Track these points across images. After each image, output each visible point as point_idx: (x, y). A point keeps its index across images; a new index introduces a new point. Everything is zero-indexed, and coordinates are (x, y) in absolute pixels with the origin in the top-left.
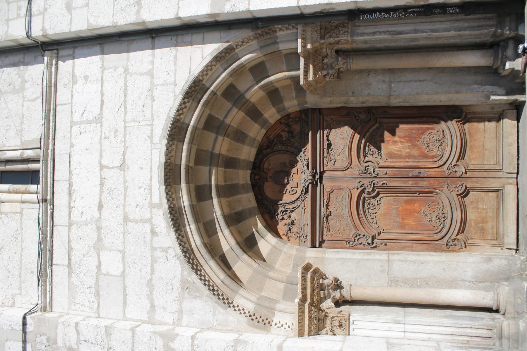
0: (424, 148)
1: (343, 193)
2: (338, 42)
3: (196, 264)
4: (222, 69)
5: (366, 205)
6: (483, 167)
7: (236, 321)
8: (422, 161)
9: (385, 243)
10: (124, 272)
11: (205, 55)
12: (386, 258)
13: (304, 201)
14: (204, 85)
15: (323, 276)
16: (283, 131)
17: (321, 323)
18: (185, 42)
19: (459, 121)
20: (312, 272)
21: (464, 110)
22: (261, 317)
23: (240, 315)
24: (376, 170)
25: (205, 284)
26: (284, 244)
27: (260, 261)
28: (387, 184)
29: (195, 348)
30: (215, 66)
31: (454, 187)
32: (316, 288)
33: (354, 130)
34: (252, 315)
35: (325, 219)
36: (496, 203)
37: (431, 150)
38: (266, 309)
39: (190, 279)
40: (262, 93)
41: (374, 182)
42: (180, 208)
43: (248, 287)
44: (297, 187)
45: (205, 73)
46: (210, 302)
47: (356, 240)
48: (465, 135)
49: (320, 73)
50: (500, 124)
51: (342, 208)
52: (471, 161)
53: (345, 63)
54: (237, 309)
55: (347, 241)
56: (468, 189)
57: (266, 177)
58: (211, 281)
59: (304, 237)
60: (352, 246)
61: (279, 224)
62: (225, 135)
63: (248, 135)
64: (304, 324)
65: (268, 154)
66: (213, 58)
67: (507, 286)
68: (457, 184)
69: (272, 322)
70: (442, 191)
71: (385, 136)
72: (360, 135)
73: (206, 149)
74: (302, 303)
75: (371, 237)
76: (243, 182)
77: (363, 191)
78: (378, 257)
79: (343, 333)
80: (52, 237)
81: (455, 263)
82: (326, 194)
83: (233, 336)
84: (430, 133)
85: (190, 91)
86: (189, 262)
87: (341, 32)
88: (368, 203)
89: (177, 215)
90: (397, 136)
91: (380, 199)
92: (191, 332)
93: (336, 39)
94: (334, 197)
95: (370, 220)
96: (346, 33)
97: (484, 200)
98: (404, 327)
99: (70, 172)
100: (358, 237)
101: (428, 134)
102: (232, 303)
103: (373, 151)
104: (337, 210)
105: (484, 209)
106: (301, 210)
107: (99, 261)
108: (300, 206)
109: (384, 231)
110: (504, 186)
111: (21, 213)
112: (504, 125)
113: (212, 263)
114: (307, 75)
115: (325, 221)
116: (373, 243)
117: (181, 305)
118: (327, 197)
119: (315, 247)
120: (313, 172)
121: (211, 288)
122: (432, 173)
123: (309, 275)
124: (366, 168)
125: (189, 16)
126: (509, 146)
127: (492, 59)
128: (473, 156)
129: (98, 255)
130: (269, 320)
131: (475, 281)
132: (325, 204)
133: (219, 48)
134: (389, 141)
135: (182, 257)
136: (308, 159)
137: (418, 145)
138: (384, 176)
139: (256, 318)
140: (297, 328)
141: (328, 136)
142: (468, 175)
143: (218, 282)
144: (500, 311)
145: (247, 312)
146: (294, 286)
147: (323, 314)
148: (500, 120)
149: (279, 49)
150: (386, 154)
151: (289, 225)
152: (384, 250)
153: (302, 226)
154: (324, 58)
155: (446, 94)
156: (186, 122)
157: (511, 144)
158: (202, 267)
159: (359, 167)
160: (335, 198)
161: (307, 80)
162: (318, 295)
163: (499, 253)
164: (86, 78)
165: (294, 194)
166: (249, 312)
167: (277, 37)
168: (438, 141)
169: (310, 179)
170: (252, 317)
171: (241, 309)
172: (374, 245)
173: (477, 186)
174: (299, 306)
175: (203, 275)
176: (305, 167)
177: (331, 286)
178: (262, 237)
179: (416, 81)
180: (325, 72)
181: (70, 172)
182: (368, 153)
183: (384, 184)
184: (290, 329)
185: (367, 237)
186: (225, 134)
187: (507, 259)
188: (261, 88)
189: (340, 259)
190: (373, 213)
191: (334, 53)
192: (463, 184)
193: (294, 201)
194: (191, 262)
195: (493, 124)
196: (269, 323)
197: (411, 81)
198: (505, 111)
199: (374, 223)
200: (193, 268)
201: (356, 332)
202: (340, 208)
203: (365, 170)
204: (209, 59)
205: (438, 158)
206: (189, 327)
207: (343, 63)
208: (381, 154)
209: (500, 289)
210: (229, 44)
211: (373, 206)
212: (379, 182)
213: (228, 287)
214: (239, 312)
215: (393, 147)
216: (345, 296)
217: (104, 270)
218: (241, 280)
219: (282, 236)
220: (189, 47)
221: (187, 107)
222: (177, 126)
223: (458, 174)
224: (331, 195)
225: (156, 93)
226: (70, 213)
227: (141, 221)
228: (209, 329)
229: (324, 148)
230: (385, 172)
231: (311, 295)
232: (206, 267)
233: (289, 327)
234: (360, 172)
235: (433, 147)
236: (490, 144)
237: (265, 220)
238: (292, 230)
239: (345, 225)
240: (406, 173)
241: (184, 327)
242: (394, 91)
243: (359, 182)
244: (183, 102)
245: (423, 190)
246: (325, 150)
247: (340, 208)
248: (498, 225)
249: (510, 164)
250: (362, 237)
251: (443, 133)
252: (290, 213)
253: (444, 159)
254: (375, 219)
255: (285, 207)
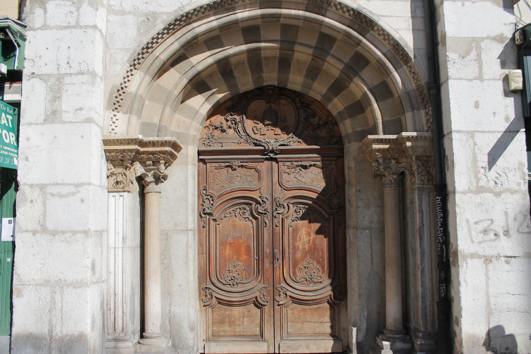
0: (303, 264)
1: (256, 182)
2: (412, 174)
3: (175, 28)
4: (385, 51)
5: (243, 206)
6: (285, 321)
7: (116, 73)
8: (290, 262)
9: (205, 226)
11: (400, 32)
12: (190, 228)
13: (247, 142)
14: (368, 32)
15: (168, 164)
16: (320, 119)
17: (119, 163)
18: (415, 10)
19: (331, 298)
20: (171, 151)
21: (343, 302)
22: (122, 99)
23: (123, 77)
24: (281, 215)
25: (153, 39)
26: (200, 122)
27: (181, 97)
28: (265, 227)
29: (84, 29)
30: (389, 43)
31: (264, 294)
32: (155, 156)
33: (321, 192)
34: (124, 90)
35: (228, 164)
36: (250, 334)
37: (302, 270)
38: (131, 104)
39: (158, 22)
40: (359, 95)
41: (268, 213)
42: (234, 9)
43: (154, 85)
44: (260, 135)
45: (381, 33)
46: (134, 45)
47: (207, 197)
48: (317, 304)
49: (380, 156)
50: (329, 337)
51: (240, 181)
52: (290, 310)
53: (391, 182)
54: (129, 74)
55: (206, 188)
56: (262, 308)
57: (271, 102)
58: (157, 45)
59: (209, 143)
60: (201, 193)
61: (222, 117)
62: (315, 57)
63: (315, 82)
64: (116, 145)
65: (295, 104)
66: (397, 41)
67: (166, 346)
68: (267, 297)
69: (118, 112)
70: (260, 282)
71: (315, 224)
72: (316, 199)
73: (298, 35)
74: (138, 142)
75: (211, 212)
76: (264, 77)
77: (258, 202)
78: (191, 219)
79: (110, 186)
81: (188, 296)
82: (254, 164)
83: (99, 70)
84: (318, 269)
85: (361, 17)
86: (176, 20)
87: (423, 178)
88: (245, 208)
89: (227, 5)
90: (315, 236)
91: (251, 221)
92: (102, 25)
93: (416, 172)
94: (251, 173)
95: (229, 211)
96: (422, 183)
97: (251, 323)
98: (120, 247)
100: (211, 199)
101: (318, 267)
102: (135, 69)
103: (299, 211)
104: (238, 176)
105: (243, 323)
106: (237, 139)
108: (241, 138)
109: (217, 225)
110: (266, 342)
112: (327, 341)
113: (176, 46)
114: (379, 142)
115: (226, 164)
116: (205, 214)
117: (130, 13)
118: (251, 166)
119: (199, 155)
120: (276, 150)
121: (150, 46)
122: (278, 272)
123: (168, 149)
124: (282, 205)
125: (445, 13)
126: (307, 346)
127: (393, 328)
128: (296, 312)
130: (119, 108)
131: (170, 316)
132: (244, 164)
133: (407, 47)
134: (310, 228)
135: (181, 13)
136: (290, 146)
137: (307, 257)
138: (274, 224)
139: (120, 95)
140: (112, 138)
141: (314, 165)
142: (277, 307)
143: (157, 52)
144: (142, 339)
145: (126, 85)
146: (156, 133)
147: (128, 165)
148: (332, 337)
149: (406, 113)
150: (296, 226)
151: (221, 127)
152: (199, 226)
153: (220, 140)
154: (396, 160)
155: (358, 285)
156: (327, 13)
157: (309, 347)
158: (172, 34)
159: (283, 198)
160: (250, 174)
161: (372, 143)
162: (148, 159)
163: (200, 338)
165: (253, 131)
166: (126, 87)
167: (419, 110)
168: (310, 277)
169: (269, 148)
170: (121, 90)
171: (129, 79)
172: (203, 216)
173: (266, 316)
174: (135, 139)
175: (164, 36)
176: (282, 143)
177: (157, 171)
178: (207, 99)
179: (371, 254)
180: (381, 161)
182: (297, 207)
183: (266, 224)
184: (110, 130)
185: (211, 207)
186: (315, 56)
187: (194, 345)
188: (365, 94)
189: (186, 180)
190: (235, 214)
191: (401, 170)
192: (268, 303)
193: (246, 132)
194: (177, 23)
195: (329, 330)
196: (116, 109)
197: (372, 249)
198: (341, 341)
199: (225, 215)
200: (170, 25)
201: (112, 200)
202: (240, 180)
203: (280, 205)
204: (396, 36)
205: (293, 278)
206: (107, 23)
207: (391, 180)
208: (297, 221)
209: (164, 339)
210: (413, 59)
211: (243, 213)
212: (268, 219)
213: (152, 64)
214: (125, 76)
215: (304, 233)
216: (148, 187)
218: (160, 78)
219: (209, 120)
220: (409, 15)
221: (344, 13)
222: (323, 3)
223: (277, 298)
224: (253, 170)
228: (106, 45)
229: (303, 162)
230: (278, 225)
231: (147, 152)
232: (172, 39)
233: (113, 130)
234: (278, 200)
235: (304, 273)
236: (308, 328)
237: (225, 102)
238: (216, 130)
239: (222, 185)
240: (277, 246)
241: (107, 18)
242: (361, 233)
243: (267, 199)
244: (349, 9)
245: (260, 264)
246: (300, 163)
247: (240, 180)
248: (228, 337)
249: (289, 347)
250: (211, 203)
251: (319, 282)
252: (234, 127)
253: (292, 284)
254: (230, 215)
255: (240, 122)
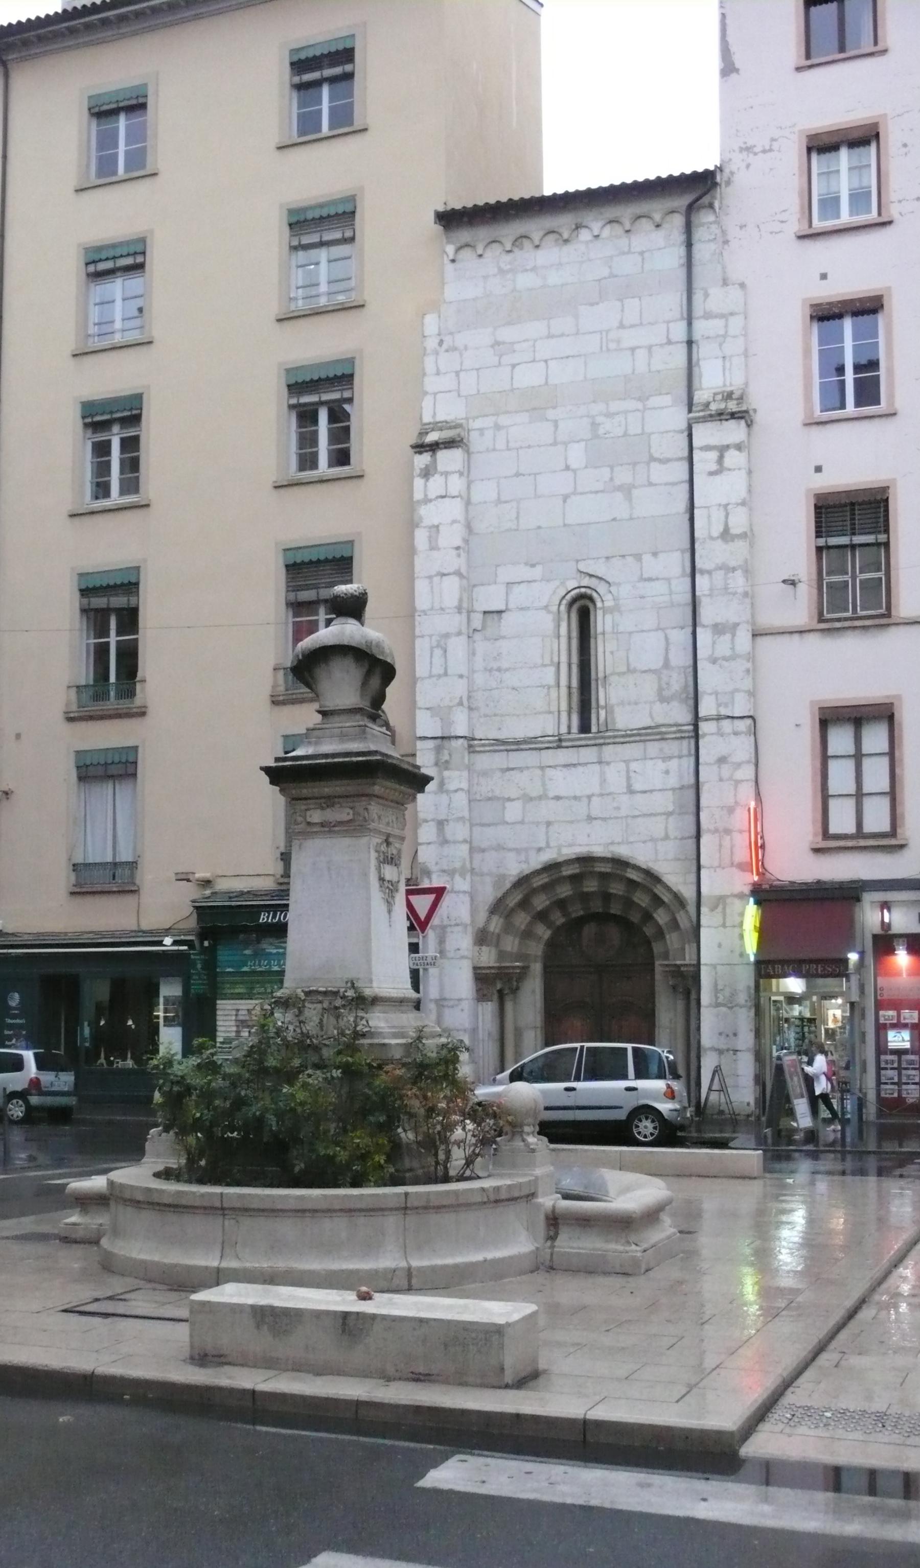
10: (507, 823)
80: (530, 749)
99: (586, 764)
107: (513, 800)
111: (550, 712)
117: (487, 874)
129: (518, 799)
164: (667, 772)
181: (586, 764)
217: (508, 804)
225: (650, 844)
226: (550, 767)
227: (548, 838)
